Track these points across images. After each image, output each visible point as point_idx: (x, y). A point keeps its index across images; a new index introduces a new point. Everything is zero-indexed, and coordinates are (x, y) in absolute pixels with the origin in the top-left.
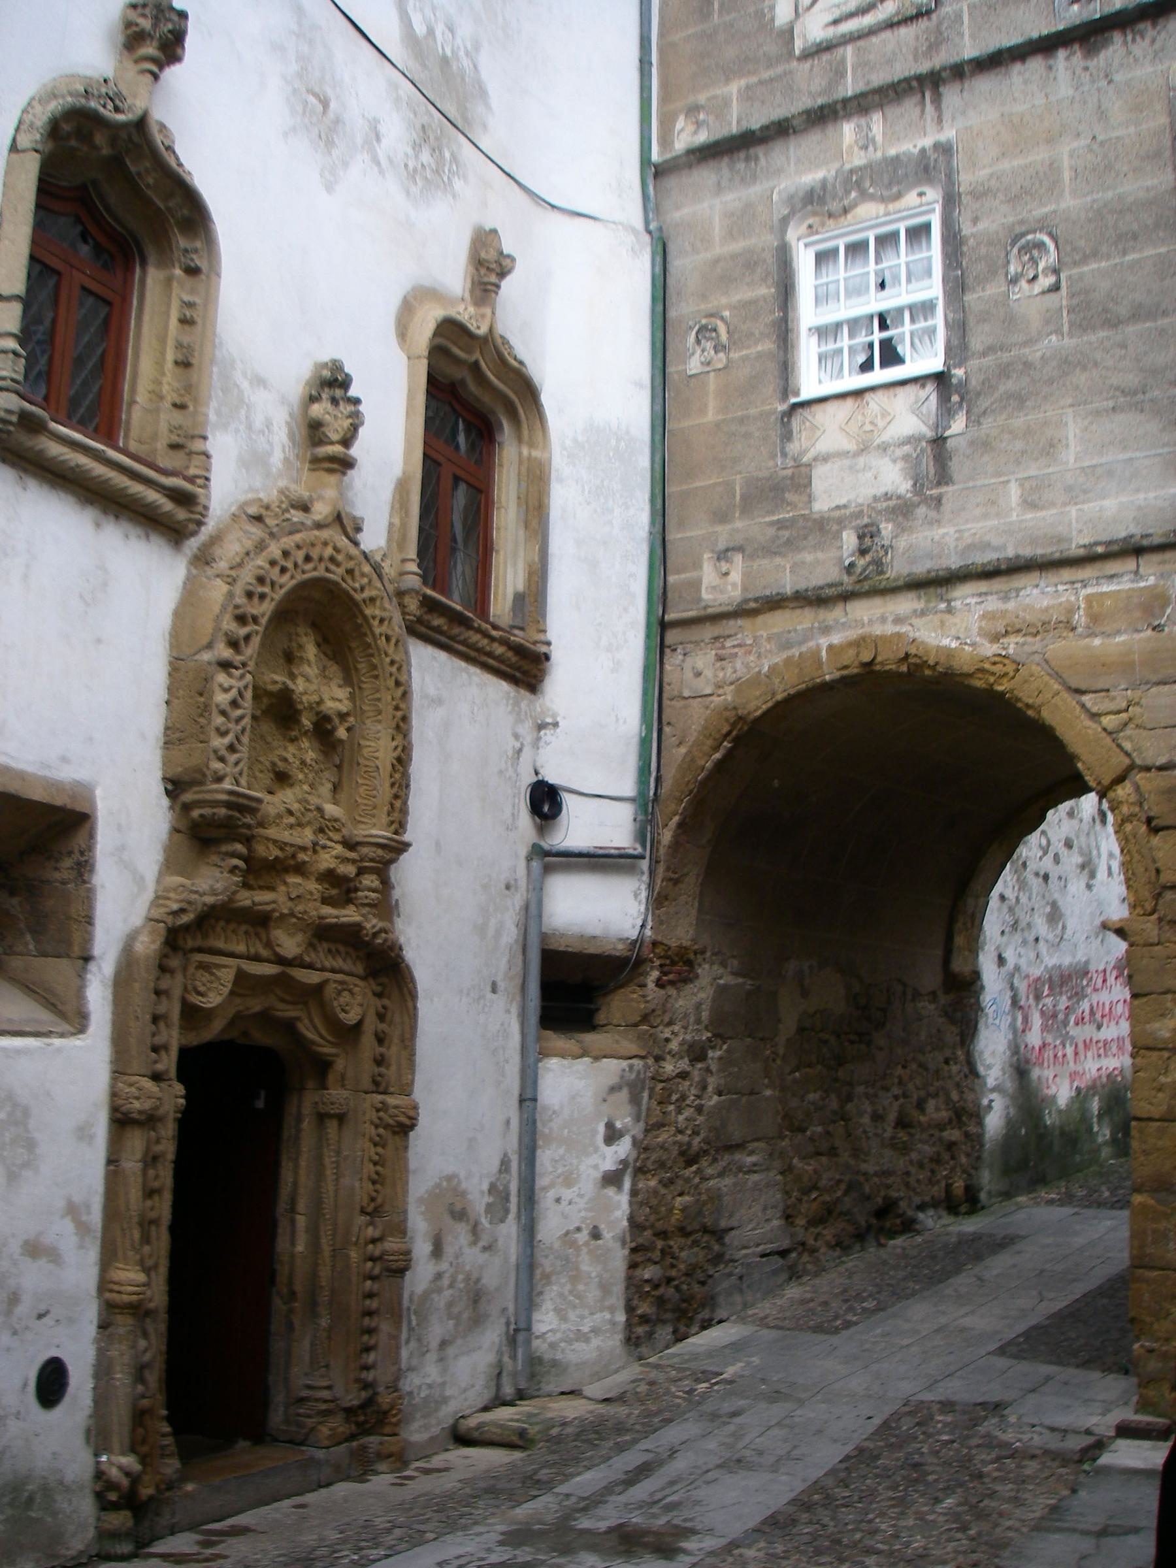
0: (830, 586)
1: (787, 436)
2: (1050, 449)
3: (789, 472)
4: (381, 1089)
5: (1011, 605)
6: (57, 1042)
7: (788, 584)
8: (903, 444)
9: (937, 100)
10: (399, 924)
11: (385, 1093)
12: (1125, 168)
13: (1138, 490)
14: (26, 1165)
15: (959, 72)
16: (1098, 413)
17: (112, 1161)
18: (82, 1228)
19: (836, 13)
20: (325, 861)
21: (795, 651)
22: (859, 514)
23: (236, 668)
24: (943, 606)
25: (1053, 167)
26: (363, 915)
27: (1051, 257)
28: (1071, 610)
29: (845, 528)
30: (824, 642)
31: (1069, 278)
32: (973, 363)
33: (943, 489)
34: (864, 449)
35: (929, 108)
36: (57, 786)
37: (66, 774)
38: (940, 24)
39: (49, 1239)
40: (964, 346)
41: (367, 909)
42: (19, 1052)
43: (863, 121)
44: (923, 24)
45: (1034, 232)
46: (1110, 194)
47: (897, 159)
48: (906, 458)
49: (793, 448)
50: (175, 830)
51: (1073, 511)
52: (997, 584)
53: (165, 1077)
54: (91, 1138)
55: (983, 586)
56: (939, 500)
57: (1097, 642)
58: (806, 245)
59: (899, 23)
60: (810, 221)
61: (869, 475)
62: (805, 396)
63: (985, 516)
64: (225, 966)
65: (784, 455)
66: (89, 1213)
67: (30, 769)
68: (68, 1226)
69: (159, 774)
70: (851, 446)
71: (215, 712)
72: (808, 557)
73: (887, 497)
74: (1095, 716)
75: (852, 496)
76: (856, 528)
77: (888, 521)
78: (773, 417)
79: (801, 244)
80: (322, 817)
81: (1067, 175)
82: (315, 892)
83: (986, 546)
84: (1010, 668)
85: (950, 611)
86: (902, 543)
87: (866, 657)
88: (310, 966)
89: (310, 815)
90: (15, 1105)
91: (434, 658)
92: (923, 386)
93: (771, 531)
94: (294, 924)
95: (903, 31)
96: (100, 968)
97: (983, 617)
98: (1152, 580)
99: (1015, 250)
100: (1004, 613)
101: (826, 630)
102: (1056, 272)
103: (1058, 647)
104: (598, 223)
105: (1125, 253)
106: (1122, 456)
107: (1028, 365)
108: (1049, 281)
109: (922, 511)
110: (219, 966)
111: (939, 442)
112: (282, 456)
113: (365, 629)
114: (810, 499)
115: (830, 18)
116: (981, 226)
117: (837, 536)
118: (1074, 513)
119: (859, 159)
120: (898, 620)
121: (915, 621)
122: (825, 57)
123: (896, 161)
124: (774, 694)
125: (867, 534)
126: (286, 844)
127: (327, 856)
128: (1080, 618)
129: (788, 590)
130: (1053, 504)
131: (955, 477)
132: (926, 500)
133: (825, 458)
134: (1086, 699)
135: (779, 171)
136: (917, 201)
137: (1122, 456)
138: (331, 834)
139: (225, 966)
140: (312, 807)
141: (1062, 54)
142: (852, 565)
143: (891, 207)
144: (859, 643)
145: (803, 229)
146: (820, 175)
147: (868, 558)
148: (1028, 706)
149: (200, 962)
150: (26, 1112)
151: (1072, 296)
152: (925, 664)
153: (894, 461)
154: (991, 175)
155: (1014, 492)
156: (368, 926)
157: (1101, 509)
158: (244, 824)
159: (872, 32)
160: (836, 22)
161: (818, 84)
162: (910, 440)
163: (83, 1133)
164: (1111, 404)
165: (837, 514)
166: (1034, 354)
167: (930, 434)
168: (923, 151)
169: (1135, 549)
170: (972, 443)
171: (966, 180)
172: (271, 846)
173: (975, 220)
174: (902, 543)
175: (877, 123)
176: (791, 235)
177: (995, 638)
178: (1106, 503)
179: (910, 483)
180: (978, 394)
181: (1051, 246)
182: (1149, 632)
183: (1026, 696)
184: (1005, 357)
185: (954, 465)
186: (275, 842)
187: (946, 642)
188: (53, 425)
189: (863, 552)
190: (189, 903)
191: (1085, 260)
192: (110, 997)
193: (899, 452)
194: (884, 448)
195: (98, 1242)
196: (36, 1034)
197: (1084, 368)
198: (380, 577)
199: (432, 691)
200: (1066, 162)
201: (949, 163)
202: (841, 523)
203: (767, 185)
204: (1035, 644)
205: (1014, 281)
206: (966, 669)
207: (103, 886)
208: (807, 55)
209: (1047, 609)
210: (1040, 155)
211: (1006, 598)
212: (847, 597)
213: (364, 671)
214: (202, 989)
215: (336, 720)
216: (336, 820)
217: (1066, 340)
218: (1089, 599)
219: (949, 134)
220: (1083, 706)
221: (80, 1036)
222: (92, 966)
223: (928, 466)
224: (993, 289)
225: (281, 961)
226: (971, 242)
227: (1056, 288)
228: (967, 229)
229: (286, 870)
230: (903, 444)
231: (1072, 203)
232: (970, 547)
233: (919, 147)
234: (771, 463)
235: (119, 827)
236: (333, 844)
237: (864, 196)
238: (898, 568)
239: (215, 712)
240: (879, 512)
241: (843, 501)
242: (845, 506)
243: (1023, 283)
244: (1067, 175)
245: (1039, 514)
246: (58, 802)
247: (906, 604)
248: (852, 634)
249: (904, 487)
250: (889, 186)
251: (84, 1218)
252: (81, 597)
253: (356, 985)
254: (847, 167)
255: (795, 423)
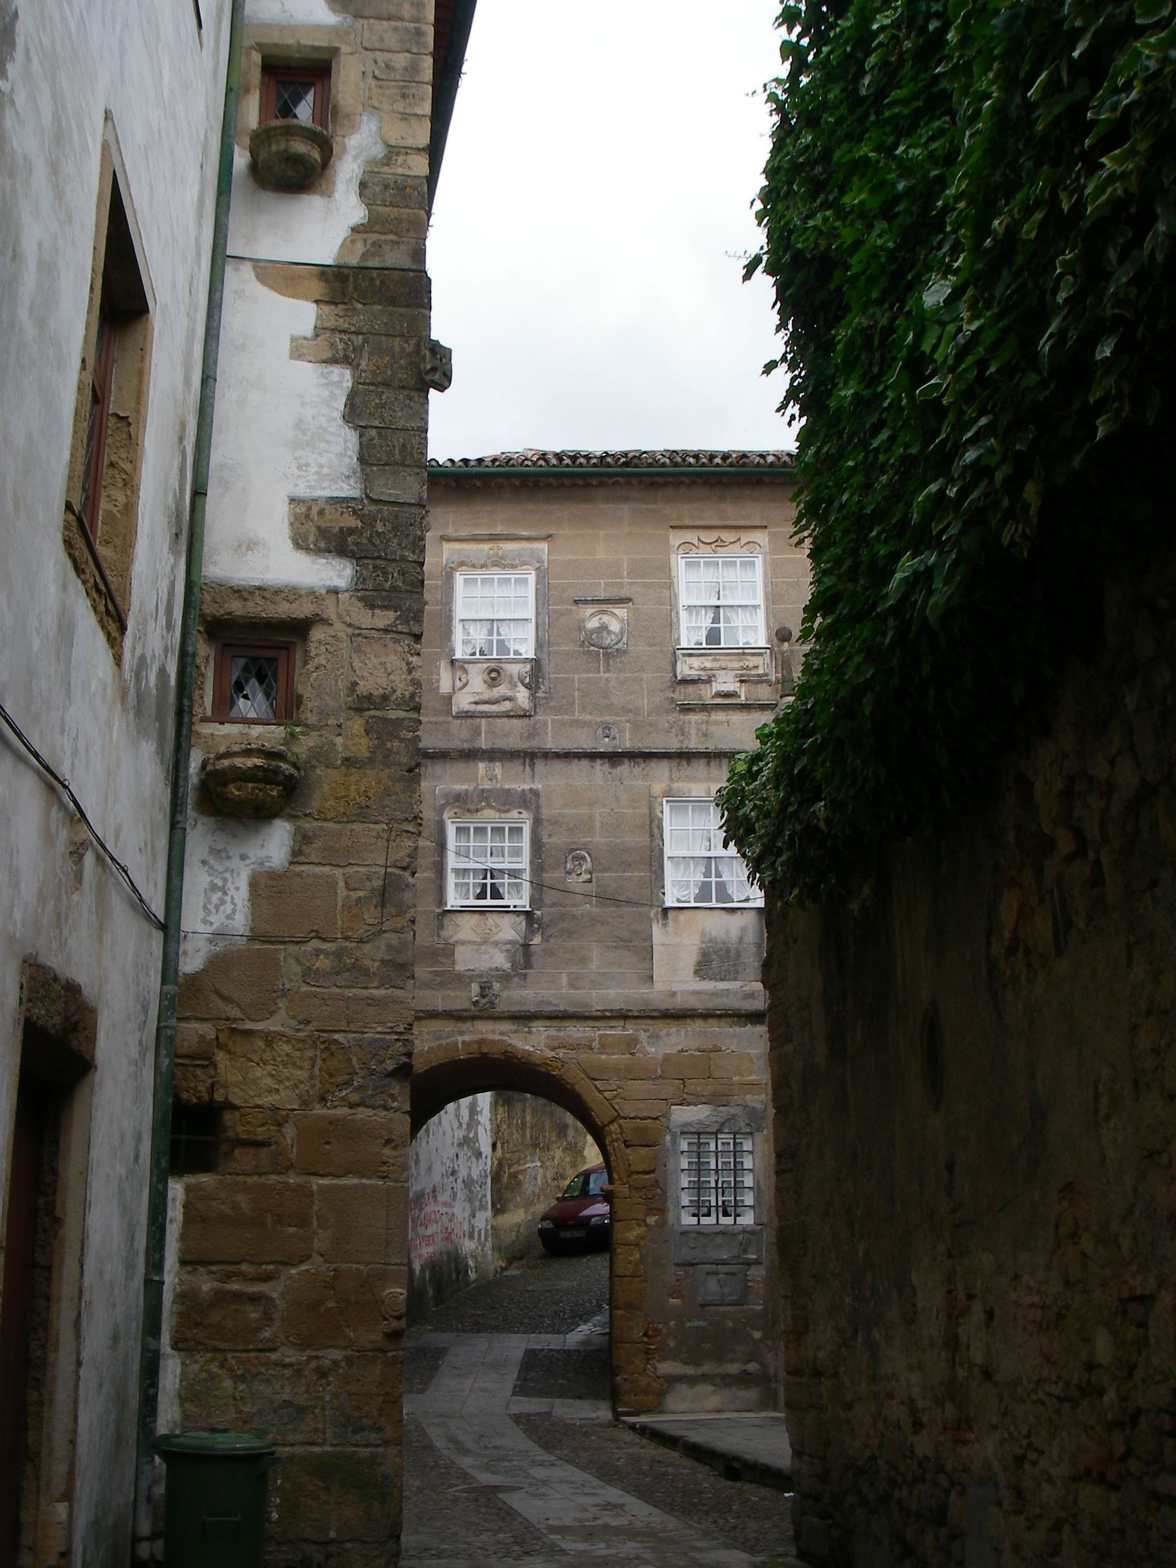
0: (465, 1010)
1: (441, 927)
2: (584, 960)
3: (442, 946)
5: (562, 1034)
7: (440, 1005)
8: (507, 943)
9: (532, 765)
12: (627, 829)
13: (625, 988)
15: (547, 755)
16: (608, 948)
19: (477, 698)
21: (444, 1042)
22: (481, 976)
24: (526, 1029)
25: (591, 818)
27: (588, 865)
28: (592, 1041)
29: (473, 982)
30: (460, 1039)
31: (597, 877)
32: (546, 909)
33: (528, 971)
34: (485, 942)
35: (527, 768)
38: (535, 724)
40: (541, 900)
43: (491, 765)
44: (526, 721)
45: (580, 850)
46: (619, 840)
47: (508, 791)
48: (508, 951)
49: (444, 933)
51: (594, 993)
52: (555, 1023)
55: (548, 1023)
56: (525, 976)
57: (603, 1057)
58: (452, 822)
59: (513, 716)
60: (456, 810)
61: (487, 956)
62: (449, 908)
63: (549, 988)
65: (439, 936)
70: (478, 940)
72: (452, 994)
73: (497, 969)
74: (600, 1091)
75: (477, 966)
76: (480, 983)
77: (497, 982)
78: (432, 915)
79: (450, 821)
81: (598, 825)
83: (550, 1003)
84: (559, 1064)
85: (530, 1032)
86: (505, 994)
87: (485, 1050)
92: (518, 916)
93: (430, 976)
95: (515, 721)
97: (547, 1038)
98: (631, 1032)
99: (570, 857)
100: (558, 1037)
101: (461, 1033)
102: (591, 873)
103: (584, 1056)
104: (115, 667)
105: (624, 872)
106: (619, 970)
107: (574, 917)
108: (586, 877)
109: (516, 980)
111: (526, 946)
114: (454, 962)
115: (473, 700)
116: (553, 839)
117: (469, 984)
118: (594, 994)
119: (487, 785)
120: (502, 1033)
121: (511, 1035)
122: (469, 721)
123: (508, 792)
124: (431, 1062)
125: (485, 989)
128: (596, 1044)
129: (440, 1009)
130: (584, 988)
131: (535, 966)
132: (518, 975)
133: (463, 943)
134: (596, 1082)
135: (439, 778)
136: (518, 816)
137: (619, 970)
141: (599, 762)
142: (477, 1001)
143: (503, 815)
144: (480, 1042)
145: (451, 814)
146: (464, 787)
147: (486, 1000)
148: (568, 1083)
151: (598, 887)
152: (516, 1057)
153: (502, 952)
154: (559, 814)
155: (564, 979)
157: (608, 994)
159: (498, 716)
160: (476, 703)
161: (465, 734)
162: (509, 942)
164: (614, 944)
165: (468, 973)
166: (578, 911)
167: (521, 941)
168: (524, 790)
169: (624, 1016)
170: (544, 950)
171: (545, 813)
173: (550, 836)
174: (505, 994)
175: (498, 769)
176: (445, 816)
177: (553, 1049)
178: (610, 991)
179: (510, 965)
180: (548, 926)
181: (589, 860)
182: (629, 1055)
183: (569, 1078)
184: (563, 910)
185: (534, 959)
187: (527, 1047)
189: (483, 996)
191: (605, 870)
193: (505, 948)
194: (496, 944)
197: (603, 924)
200: (598, 818)
201: (538, 801)
202: (472, 979)
203: (432, 783)
204: (573, 1054)
205: (569, 873)
206: (537, 1062)
208: (458, 717)
209: (578, 1039)
210: (585, 811)
211: (559, 1030)
212: (474, 1018)
217: (594, 909)
218: (601, 1036)
219: (538, 786)
220: (596, 1086)
223: (520, 958)
224: (558, 874)
226: (547, 846)
227: (590, 881)
228: (545, 840)
230: (507, 943)
231: (599, 839)
232: (542, 1002)
233: (522, 788)
234: (430, 940)
237: (489, 806)
238: (502, 1006)
240: (493, 976)
241: (472, 968)
242: (473, 970)
243: (574, 875)
244: (598, 825)
245: (577, 991)
247: (506, 1026)
248: (476, 1037)
249: (507, 966)
250: (504, 804)
254: (481, 787)
255: (446, 920)
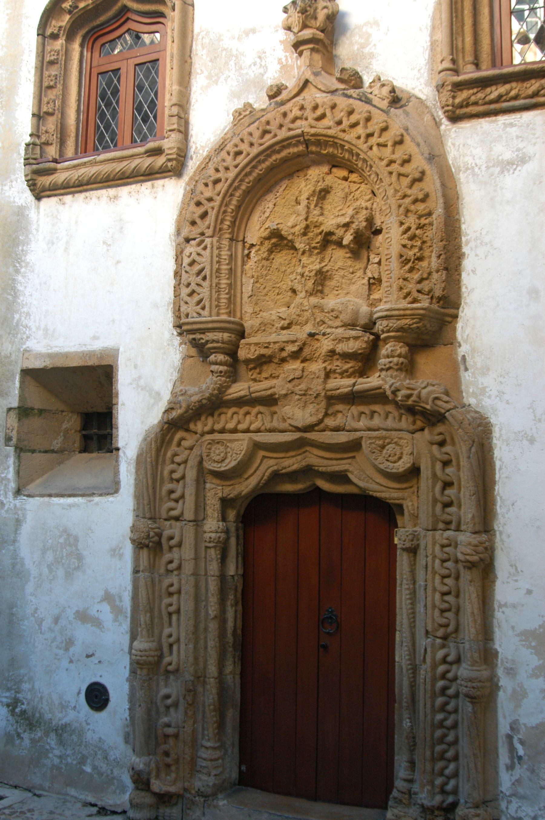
4: (453, 526)
6: (97, 499)
10: (466, 377)
11: (458, 529)
14: (78, 568)
17: (136, 571)
18: (117, 610)
20: (326, 345)
23: (194, 239)
26: (383, 380)
36: (91, 354)
37: (97, 346)
39: (93, 612)
41: (384, 373)
42: (70, 506)
50: (186, 358)
53: (181, 519)
54: (121, 556)
64: (237, 440)
66: (121, 601)
67: (73, 350)
68: (106, 608)
69: (171, 326)
71: (183, 273)
80: (323, 311)
82: (317, 371)
88: (337, 429)
89: (307, 314)
90: (69, 535)
91: (512, 125)
94: (299, 400)
96: (124, 453)
110: (230, 441)
112: (279, 67)
113: (355, 150)
126: (269, 343)
127: (326, 341)
138: (330, 323)
139: (237, 440)
140: (307, 308)
149: (213, 440)
150: (76, 539)
156: (387, 387)
158: (207, 342)
163: (115, 552)
172: (253, 348)
186: (256, 344)
188: (59, 166)
190: (175, 403)
192: (133, 470)
195: (129, 620)
196: (83, 495)
198: (368, 102)
199: (508, 155)
207: (123, 404)
213: (375, 180)
214: (217, 458)
215: (340, 232)
216: (333, 311)
221: (116, 495)
222: (121, 453)
225: (298, 429)
229: (283, 360)
235: (136, 367)
236: (334, 329)
239: (183, 273)
246: (90, 363)
251: (117, 603)
252: (104, 243)
253: (401, 438)
